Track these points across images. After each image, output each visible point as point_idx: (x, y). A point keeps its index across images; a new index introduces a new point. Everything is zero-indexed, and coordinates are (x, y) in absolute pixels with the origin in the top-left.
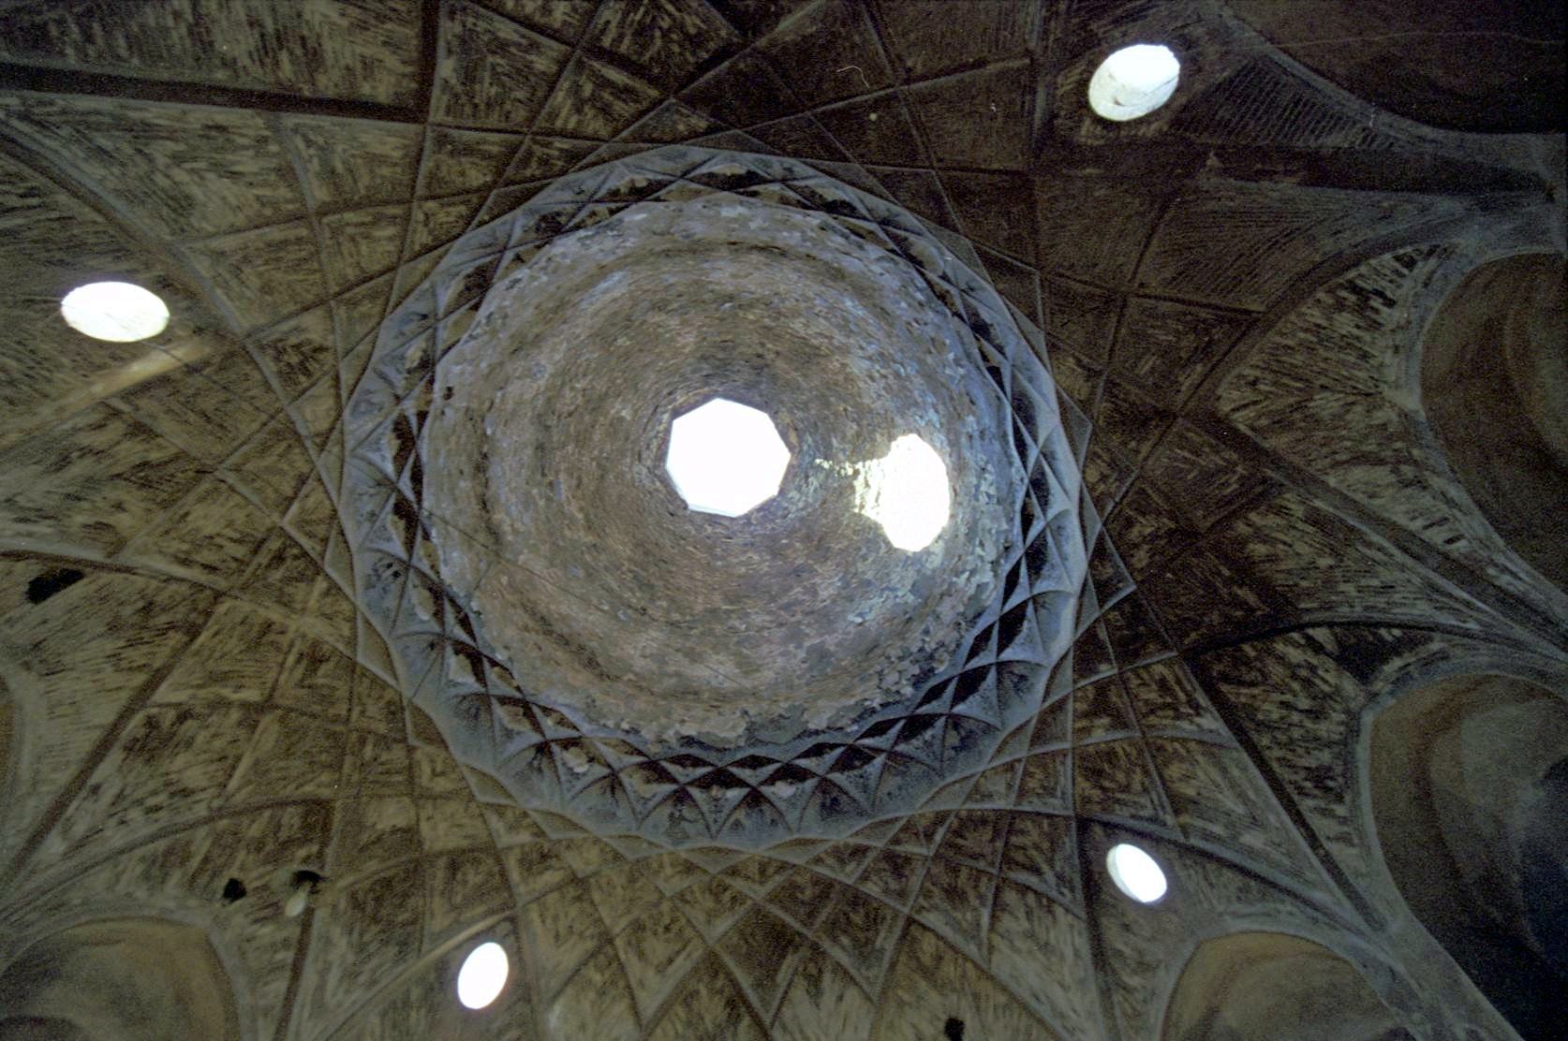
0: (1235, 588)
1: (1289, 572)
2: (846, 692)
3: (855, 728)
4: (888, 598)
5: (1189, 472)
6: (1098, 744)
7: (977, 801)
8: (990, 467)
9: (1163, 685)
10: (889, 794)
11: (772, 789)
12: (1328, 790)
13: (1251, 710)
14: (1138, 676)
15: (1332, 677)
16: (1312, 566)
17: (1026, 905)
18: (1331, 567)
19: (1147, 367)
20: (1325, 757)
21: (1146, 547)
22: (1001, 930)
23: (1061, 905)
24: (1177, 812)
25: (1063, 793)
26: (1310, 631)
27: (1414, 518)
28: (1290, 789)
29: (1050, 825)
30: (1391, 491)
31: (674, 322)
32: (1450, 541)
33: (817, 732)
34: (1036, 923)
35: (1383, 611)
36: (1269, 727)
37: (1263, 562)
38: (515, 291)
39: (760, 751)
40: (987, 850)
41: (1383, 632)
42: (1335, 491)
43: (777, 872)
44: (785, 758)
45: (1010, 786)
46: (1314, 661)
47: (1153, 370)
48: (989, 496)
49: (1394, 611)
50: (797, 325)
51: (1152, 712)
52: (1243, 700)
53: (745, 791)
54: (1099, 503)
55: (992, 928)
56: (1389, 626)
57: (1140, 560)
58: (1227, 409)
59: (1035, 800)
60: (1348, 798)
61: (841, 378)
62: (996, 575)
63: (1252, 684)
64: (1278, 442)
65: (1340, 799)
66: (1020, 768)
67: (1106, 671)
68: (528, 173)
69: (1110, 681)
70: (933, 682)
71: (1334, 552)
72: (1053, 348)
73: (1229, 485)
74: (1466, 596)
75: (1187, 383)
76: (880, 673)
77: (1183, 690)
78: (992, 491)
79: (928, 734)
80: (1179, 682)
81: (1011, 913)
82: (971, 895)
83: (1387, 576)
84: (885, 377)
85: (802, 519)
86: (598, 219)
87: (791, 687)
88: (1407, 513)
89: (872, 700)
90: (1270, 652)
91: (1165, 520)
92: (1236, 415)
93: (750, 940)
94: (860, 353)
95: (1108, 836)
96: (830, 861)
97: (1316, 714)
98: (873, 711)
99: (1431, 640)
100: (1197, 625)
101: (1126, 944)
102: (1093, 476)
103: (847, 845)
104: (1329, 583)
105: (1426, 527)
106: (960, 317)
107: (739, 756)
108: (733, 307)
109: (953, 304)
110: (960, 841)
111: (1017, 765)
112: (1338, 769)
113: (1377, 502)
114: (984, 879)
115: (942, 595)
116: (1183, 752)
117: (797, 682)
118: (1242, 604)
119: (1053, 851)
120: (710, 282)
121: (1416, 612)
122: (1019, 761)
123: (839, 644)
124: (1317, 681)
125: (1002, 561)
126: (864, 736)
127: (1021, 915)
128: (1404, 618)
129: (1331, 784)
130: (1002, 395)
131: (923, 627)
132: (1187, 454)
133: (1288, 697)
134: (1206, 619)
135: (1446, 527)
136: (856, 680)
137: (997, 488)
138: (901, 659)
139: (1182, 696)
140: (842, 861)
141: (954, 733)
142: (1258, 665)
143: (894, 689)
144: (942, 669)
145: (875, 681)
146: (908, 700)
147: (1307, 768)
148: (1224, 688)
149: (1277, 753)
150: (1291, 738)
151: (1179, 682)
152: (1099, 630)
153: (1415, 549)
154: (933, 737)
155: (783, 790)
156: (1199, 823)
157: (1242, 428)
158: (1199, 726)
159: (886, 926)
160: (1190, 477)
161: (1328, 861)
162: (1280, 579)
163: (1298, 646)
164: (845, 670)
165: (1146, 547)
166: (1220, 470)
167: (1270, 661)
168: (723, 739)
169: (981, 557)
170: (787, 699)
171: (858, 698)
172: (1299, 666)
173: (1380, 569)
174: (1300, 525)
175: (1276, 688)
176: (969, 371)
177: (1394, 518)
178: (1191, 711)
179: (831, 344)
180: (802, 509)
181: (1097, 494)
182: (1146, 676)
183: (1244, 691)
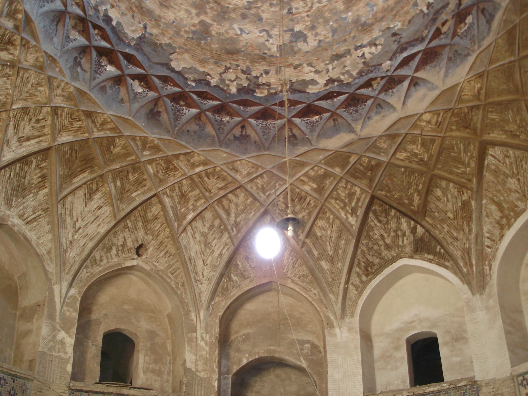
0: (416, 195)
1: (437, 207)
2: (203, 62)
3: (193, 84)
4: (263, 36)
5: (455, 153)
6: (303, 190)
7: (229, 168)
8: (379, 47)
9: (351, 195)
10: (188, 131)
11: (132, 82)
12: (367, 270)
13: (372, 228)
14: (346, 184)
15: (407, 242)
16: (446, 213)
17: (213, 222)
18: (449, 218)
19: (493, 117)
20: (376, 261)
21: (409, 154)
22: (193, 226)
23: (229, 233)
24: (307, 236)
25: (269, 195)
26: (418, 226)
27: (488, 233)
28: (356, 261)
29: (251, 202)
30: (493, 220)
32: (488, 246)
33: (172, 70)
34: (211, 233)
35: (448, 244)
36: (370, 238)
37: (435, 197)
39: (139, 57)
40: (214, 191)
41: (439, 247)
42: (481, 205)
43: (109, 129)
44: (151, 72)
45: (249, 174)
46: (407, 234)
47: (494, 119)
48: (363, 54)
49: (450, 247)
51: (336, 199)
52: (372, 223)
53: (118, 72)
55: (190, 223)
56: (442, 247)
57: (401, 156)
58: (490, 152)
59: (255, 188)
60: (369, 277)
62: (326, 85)
63: (380, 221)
64: (488, 176)
65: (367, 275)
66: (260, 171)
67: (337, 171)
69: (334, 176)
70: (249, 98)
71: (456, 217)
72: (480, 76)
73: (459, 169)
74: (474, 262)
75: (494, 135)
76: (227, 69)
77: (357, 203)
78: (367, 56)
79: (226, 119)
80: (359, 200)
81: (203, 222)
82: (191, 202)
83: (460, 236)
87: (178, 33)
88: (489, 229)
89: (212, 78)
90: (398, 219)
91: (427, 155)
92: (490, 157)
93: (74, 153)
95: (271, 221)
96: (139, 143)
97: (388, 247)
98: (208, 84)
99: (449, 261)
100: (389, 191)
101: (242, 264)
103: (152, 141)
104: (443, 221)
105: (488, 238)
107: (127, 50)
110: (206, 179)
111: (260, 169)
112: (376, 267)
113: (486, 219)
114: (203, 201)
115: (291, 65)
116: (331, 221)
117: (182, 33)
118: (411, 200)
119: (243, 211)
121: (455, 252)
122: (263, 168)
123: (219, 34)
124: (401, 239)
126: (194, 92)
127: (207, 225)
128: (450, 250)
129: (370, 269)
130: (427, 41)
131: (267, 68)
132: (462, 148)
133: (386, 235)
134: (394, 192)
135: (492, 243)
136: (212, 60)
137: (371, 58)
138: (243, 72)
139: (353, 204)
140: (144, 147)
141: (240, 130)
142: (390, 218)
143: (227, 82)
144: (259, 95)
145: (221, 70)
146: (230, 93)
147: (367, 259)
148: (371, 215)
149: (364, 248)
150: (372, 248)
151: (359, 200)
152: (352, 157)
153: (479, 240)
154: (228, 122)
155: (137, 87)
156: (311, 246)
157: (486, 162)
158: (347, 218)
159: (143, 190)
160: (452, 154)
161: (346, 290)
162: (432, 206)
163: (409, 225)
164: (211, 51)
165: (409, 154)
166: (463, 163)
167: (395, 221)
168: (125, 33)
169: (328, 71)
170: (170, 38)
171: (206, 70)
172: (401, 230)
173: (462, 232)
174: (459, 201)
175: (385, 229)
177: (484, 228)
178: (350, 211)
182: (349, 187)
183: (376, 221)
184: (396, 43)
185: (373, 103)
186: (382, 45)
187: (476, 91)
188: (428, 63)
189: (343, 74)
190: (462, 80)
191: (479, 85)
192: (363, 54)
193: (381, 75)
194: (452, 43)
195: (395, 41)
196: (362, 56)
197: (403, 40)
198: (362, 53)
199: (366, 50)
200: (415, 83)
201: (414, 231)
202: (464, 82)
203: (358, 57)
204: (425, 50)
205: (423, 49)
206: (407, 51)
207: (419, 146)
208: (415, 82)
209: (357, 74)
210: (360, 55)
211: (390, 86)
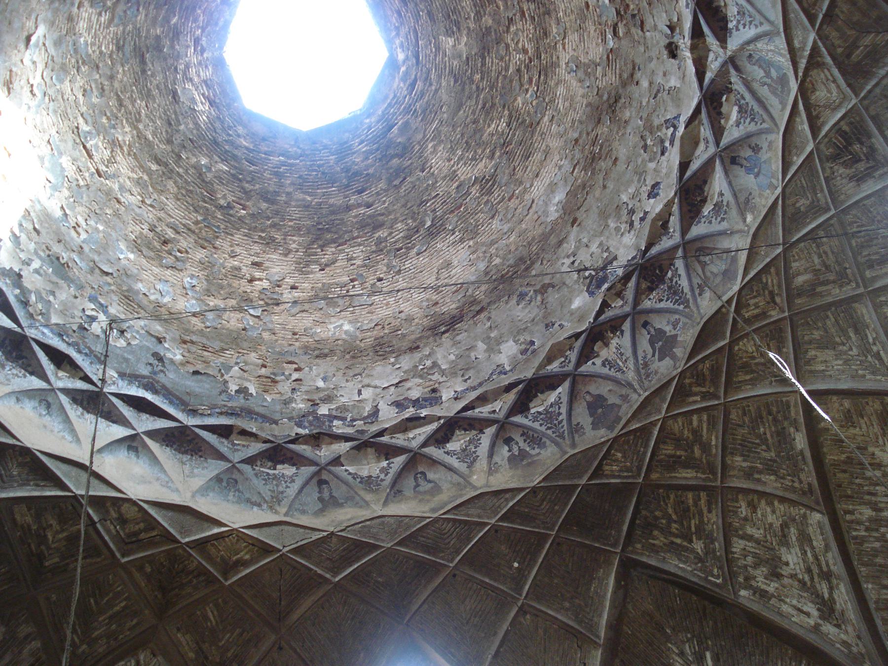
31: (466, 172)
38: (650, 182)
48: (93, 319)
50: (358, 252)
54: (98, 502)
61: (278, 237)
68: (708, 364)
84: (251, 281)
85: (178, 57)
86: (613, 291)
91: (57, 560)
94: (289, 281)
102: (129, 512)
106: (293, 441)
108: (423, 223)
109: (306, 443)
120: (462, 240)
160: (92, 601)
176: (230, 398)
179: (316, 262)
180: (187, 66)
181: (108, 504)
184: (149, 368)
186: (129, 344)
187: (235, 558)
188: (171, 446)
190: (235, 526)
191: (247, 557)
193: (90, 375)
195: (151, 364)
196: (88, 316)
197: (161, 377)
198: (94, 313)
200: (132, 443)
204: (187, 426)
205: (185, 423)
206: (155, 396)
207: (65, 534)
208: (134, 444)
210: (89, 313)
211: (85, 403)
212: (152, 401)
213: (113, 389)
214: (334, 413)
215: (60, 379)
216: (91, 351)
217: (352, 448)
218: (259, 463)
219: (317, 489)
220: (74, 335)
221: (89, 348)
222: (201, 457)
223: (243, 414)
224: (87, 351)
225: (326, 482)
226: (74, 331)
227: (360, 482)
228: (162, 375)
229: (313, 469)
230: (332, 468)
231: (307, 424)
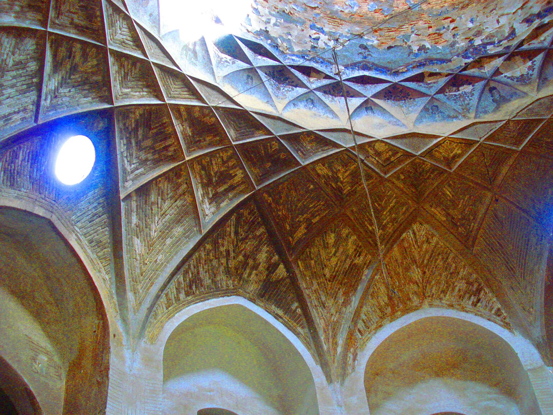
12: (191, 287)
14: (230, 158)
16: (324, 267)
18: (325, 275)
20: (207, 281)
21: (330, 174)
26: (281, 266)
28: (186, 266)
32: (360, 331)
46: (261, 268)
48: (318, 39)
52: (228, 229)
54: (361, 147)
63: (236, 233)
65: (187, 294)
71: (333, 278)
91: (349, 188)
97: (228, 272)
102: (379, 147)
104: (314, 275)
105: (363, 321)
106: (465, 69)
109: (473, 67)
113: (370, 297)
116: (180, 191)
118: (295, 227)
124: (248, 271)
125: (269, 41)
133: (232, 254)
142: (250, 236)
147: (198, 273)
157: (404, 235)
163: (269, 258)
172: (254, 259)
174: (348, 261)
176: (416, 55)
178: (211, 196)
181: (367, 147)
182: (231, 164)
184: (361, 56)
185: (306, 93)
187: (452, 155)
188: (391, 99)
189: (283, 40)
190: (446, 135)
191: (459, 152)
192: (318, 39)
193: (328, 74)
194: (435, 96)
195: (360, 53)
196: (314, 39)
198: (317, 36)
199: (323, 37)
200: (367, 106)
201: (272, 268)
202: (445, 138)
203: (310, 36)
204: (396, 83)
207: (348, 173)
208: (369, 106)
209: (299, 51)
210: (313, 37)
211: (332, 91)
212: (370, 75)
213: (344, 77)
214: (486, 41)
215: (312, 83)
216: (324, 59)
217: (505, 60)
218: (447, 90)
219: (489, 95)
220: (310, 53)
221: (322, 58)
222: (411, 99)
223: (427, 63)
224: (321, 60)
225: (494, 88)
226: (310, 51)
227: (517, 81)
228: (369, 57)
229: (483, 82)
230: (496, 78)
231: (470, 55)
